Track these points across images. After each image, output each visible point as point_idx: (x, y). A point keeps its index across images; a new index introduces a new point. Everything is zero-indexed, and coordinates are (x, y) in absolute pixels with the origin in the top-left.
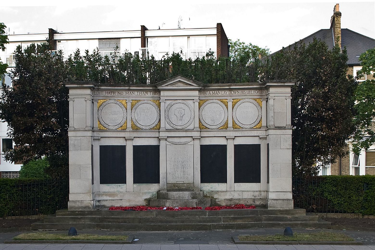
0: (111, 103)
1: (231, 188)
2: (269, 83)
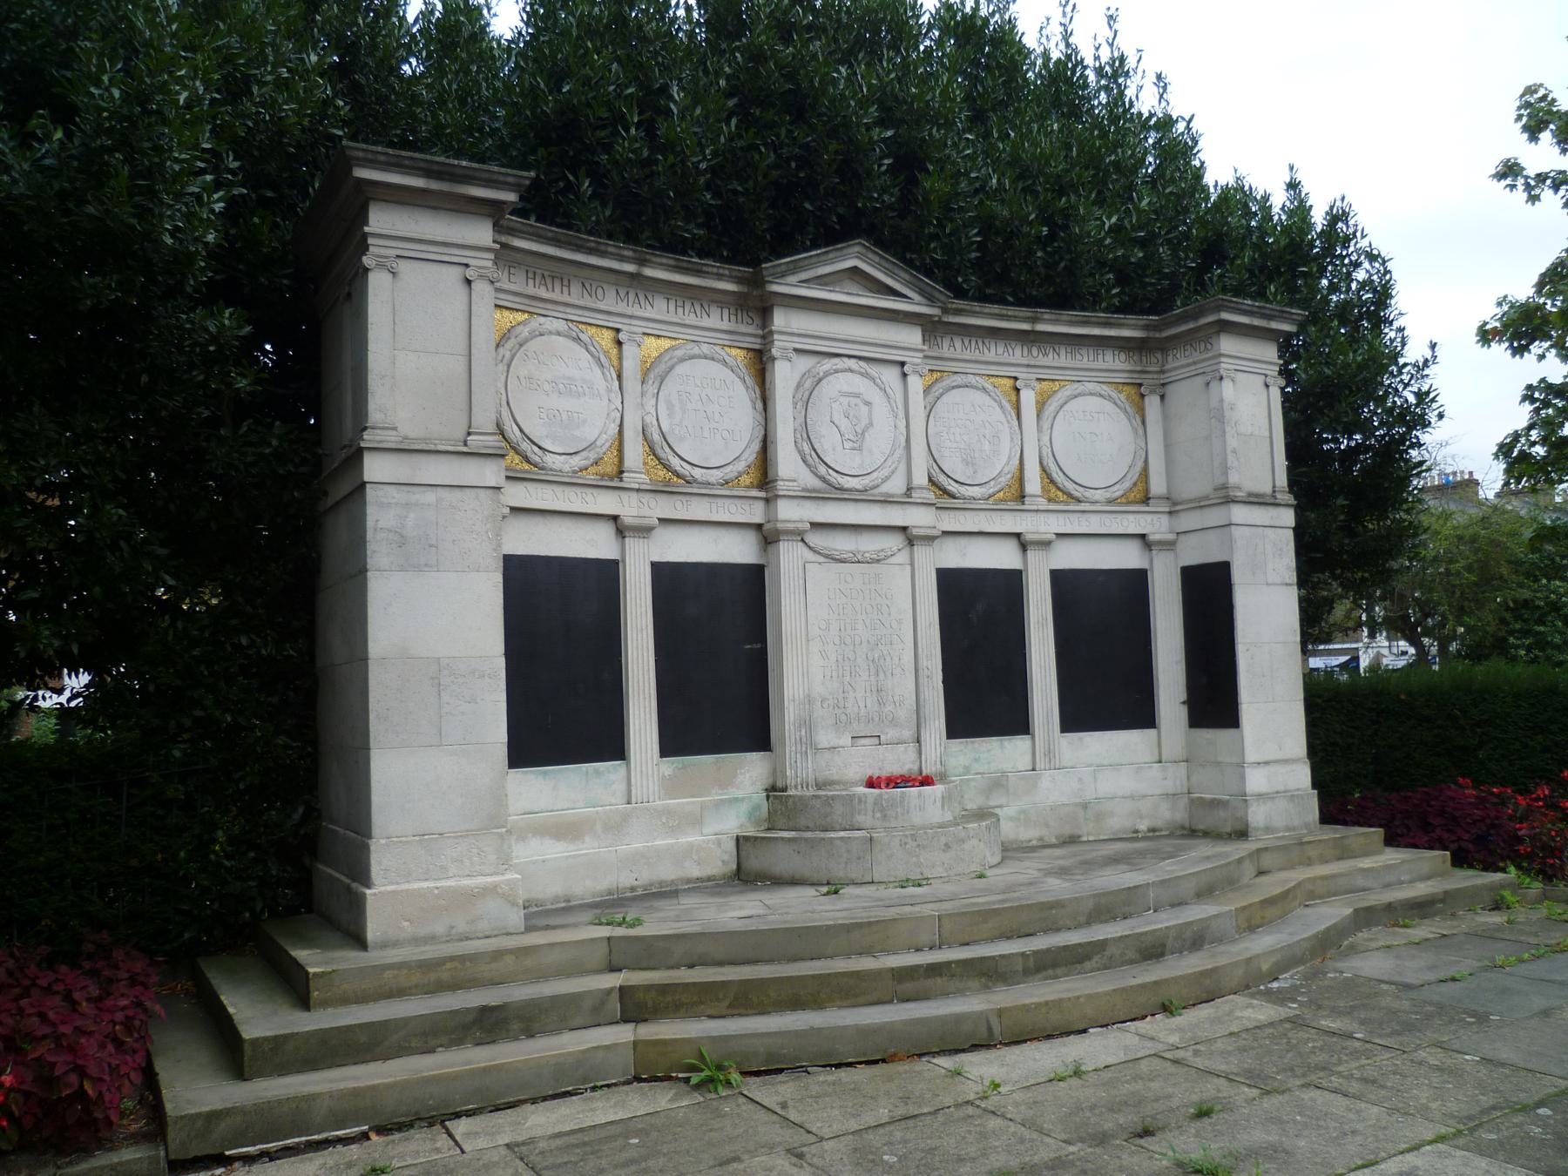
0: (551, 333)
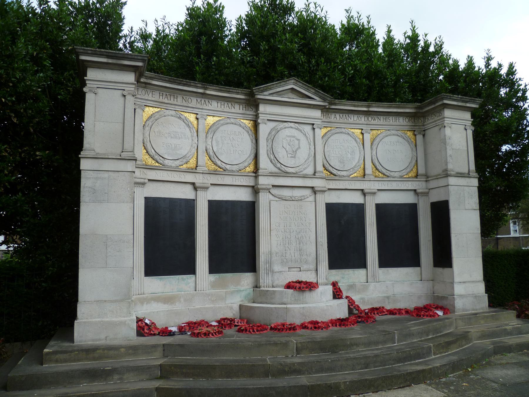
0: (169, 115)
2: (447, 99)
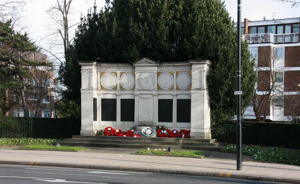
1: (175, 125)
